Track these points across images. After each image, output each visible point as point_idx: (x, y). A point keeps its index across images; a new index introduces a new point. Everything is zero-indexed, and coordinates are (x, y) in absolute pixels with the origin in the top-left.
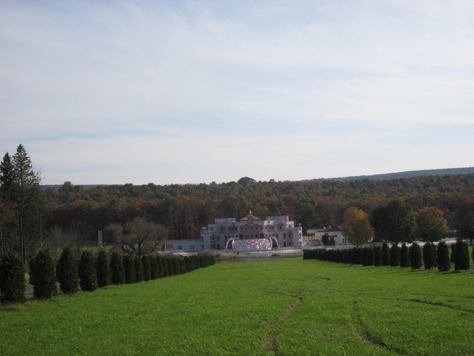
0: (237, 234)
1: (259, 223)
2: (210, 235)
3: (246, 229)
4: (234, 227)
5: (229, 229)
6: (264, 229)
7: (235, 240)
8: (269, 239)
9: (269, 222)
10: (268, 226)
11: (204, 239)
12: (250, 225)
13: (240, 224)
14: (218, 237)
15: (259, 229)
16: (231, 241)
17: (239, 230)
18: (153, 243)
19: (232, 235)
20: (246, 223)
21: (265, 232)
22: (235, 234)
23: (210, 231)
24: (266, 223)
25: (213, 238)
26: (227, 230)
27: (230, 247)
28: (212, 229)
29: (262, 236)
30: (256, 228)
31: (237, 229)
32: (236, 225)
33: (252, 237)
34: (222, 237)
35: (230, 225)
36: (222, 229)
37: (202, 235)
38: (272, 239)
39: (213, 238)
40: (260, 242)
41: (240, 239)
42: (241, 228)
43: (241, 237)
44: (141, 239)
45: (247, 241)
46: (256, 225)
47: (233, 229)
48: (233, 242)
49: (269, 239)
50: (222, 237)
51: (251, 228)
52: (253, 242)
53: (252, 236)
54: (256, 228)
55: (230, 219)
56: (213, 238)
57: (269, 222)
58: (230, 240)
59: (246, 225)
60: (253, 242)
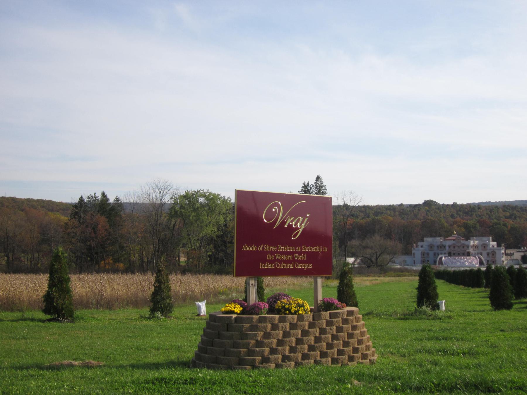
0: (445, 251)
1: (466, 243)
2: (420, 252)
3: (454, 247)
4: (443, 245)
5: (438, 247)
6: (470, 247)
7: (445, 257)
8: (476, 257)
9: (474, 242)
10: (473, 245)
11: (416, 255)
12: (457, 244)
13: (448, 243)
14: (428, 254)
15: (466, 248)
16: (441, 258)
17: (447, 248)
18: (388, 257)
19: (440, 252)
20: (453, 242)
21: (471, 251)
22: (443, 252)
23: (421, 248)
24: (472, 243)
25: (424, 255)
26: (436, 248)
27: (441, 263)
28: (422, 247)
29: (469, 254)
30: (463, 247)
31: (445, 247)
32: (444, 243)
33: (459, 255)
34: (431, 253)
35: (439, 243)
36: (431, 247)
37: (413, 252)
38: (479, 258)
39: (424, 255)
40: (468, 260)
41: (449, 256)
42: (450, 247)
43: (450, 254)
44: (378, 254)
45: (456, 258)
46: (464, 244)
47: (442, 247)
48: (443, 258)
49: (476, 257)
50: (431, 253)
51: (459, 247)
52: (462, 259)
53: (459, 254)
54: (463, 247)
55: (438, 238)
56: (423, 254)
57: (474, 242)
58: (440, 256)
59: (454, 244)
60: (462, 259)
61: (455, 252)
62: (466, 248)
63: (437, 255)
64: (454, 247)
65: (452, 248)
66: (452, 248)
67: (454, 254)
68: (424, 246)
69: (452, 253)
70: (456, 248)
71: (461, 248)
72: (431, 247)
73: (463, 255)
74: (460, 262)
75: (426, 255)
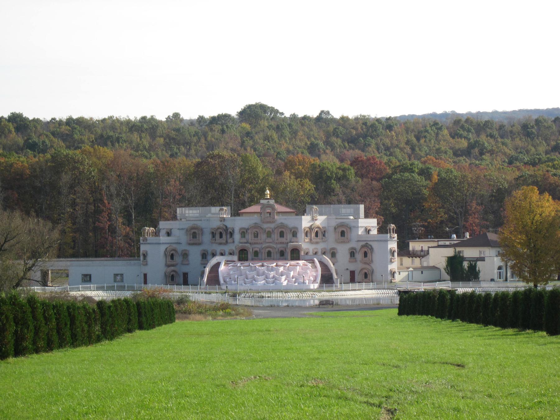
0: (231, 247)
1: (290, 221)
2: (163, 248)
3: (256, 235)
5: (213, 234)
7: (227, 263)
8: (313, 262)
9: (313, 219)
10: (311, 228)
11: (149, 258)
12: (265, 226)
13: (239, 223)
14: (185, 255)
15: (289, 236)
16: (218, 265)
18: (19, 266)
19: (219, 249)
20: (255, 219)
21: (304, 244)
22: (227, 248)
23: (163, 238)
24: (306, 221)
25: (172, 257)
26: (207, 237)
27: (214, 280)
28: (169, 234)
29: (295, 254)
30: (282, 234)
31: (231, 234)
32: (229, 225)
34: (195, 253)
35: (216, 224)
36: (194, 234)
37: (143, 248)
38: (321, 263)
39: (172, 257)
40: (289, 270)
41: (240, 259)
42: (243, 233)
43: (243, 255)
45: (258, 265)
46: (282, 226)
47: (223, 233)
48: (222, 268)
49: (313, 262)
50: (195, 253)
51: (269, 234)
52: (272, 269)
53: (269, 254)
54: (282, 234)
55: (215, 210)
56: (171, 255)
57: (313, 219)
58: (213, 261)
59: (256, 226)
61: (257, 247)
62: (289, 236)
63: (209, 257)
64: (256, 235)
65: (250, 237)
66: (250, 237)
67: (256, 254)
68: (175, 232)
69: (250, 251)
70: (263, 237)
71: (276, 236)
72: (194, 235)
73: (282, 255)
74: (267, 277)
75: (178, 259)
